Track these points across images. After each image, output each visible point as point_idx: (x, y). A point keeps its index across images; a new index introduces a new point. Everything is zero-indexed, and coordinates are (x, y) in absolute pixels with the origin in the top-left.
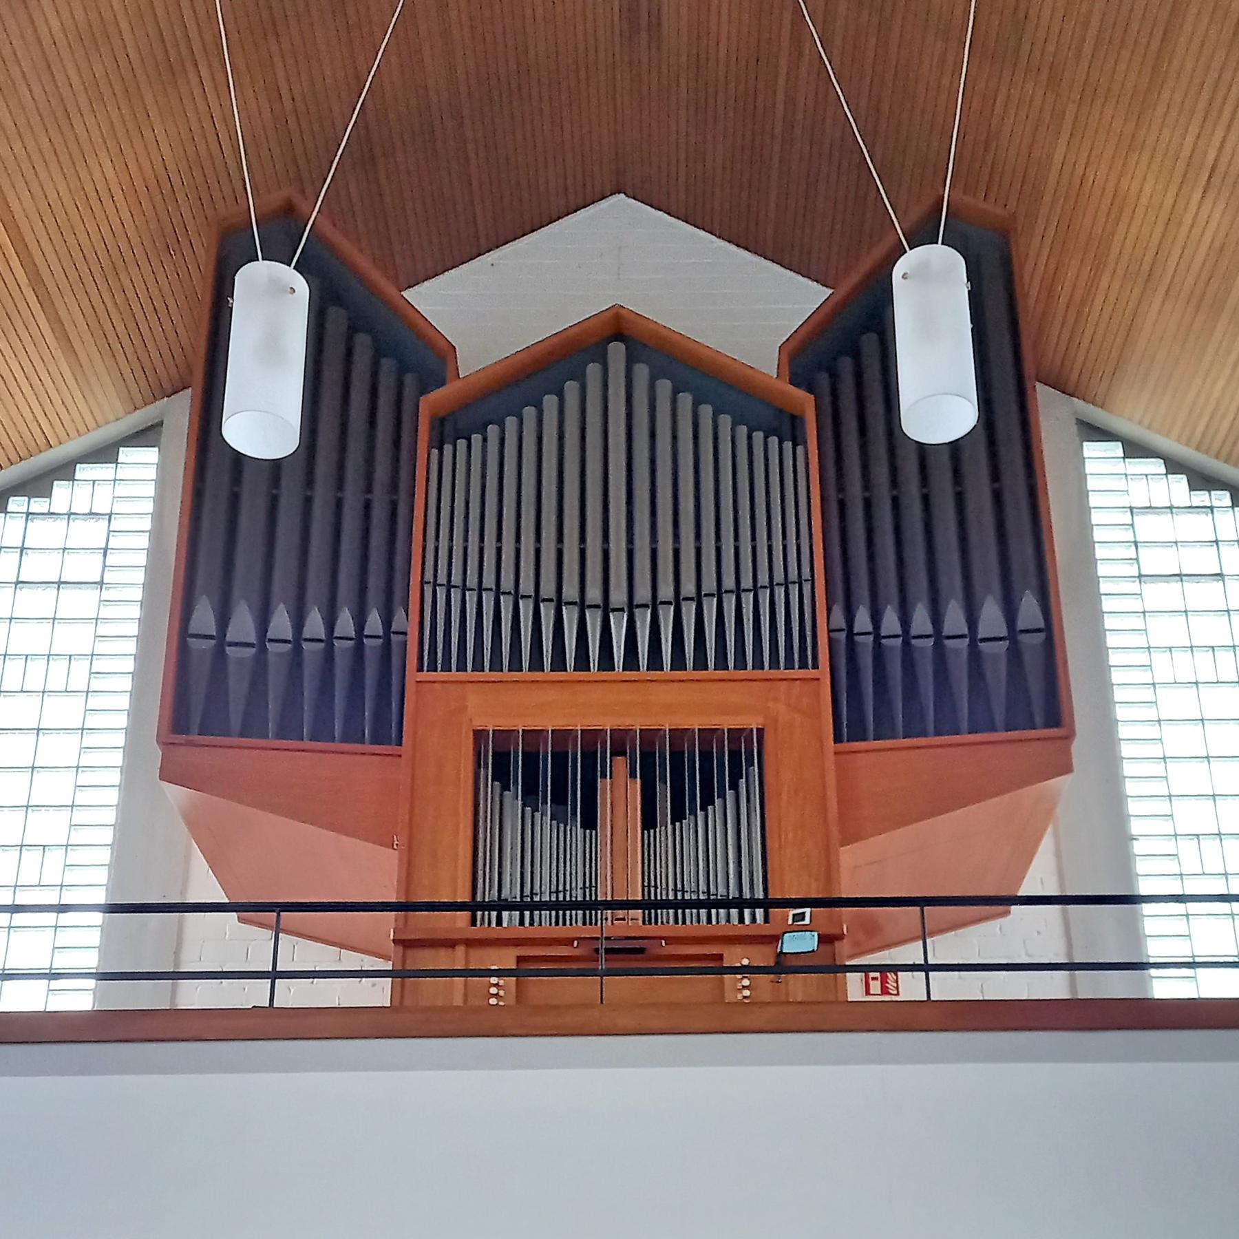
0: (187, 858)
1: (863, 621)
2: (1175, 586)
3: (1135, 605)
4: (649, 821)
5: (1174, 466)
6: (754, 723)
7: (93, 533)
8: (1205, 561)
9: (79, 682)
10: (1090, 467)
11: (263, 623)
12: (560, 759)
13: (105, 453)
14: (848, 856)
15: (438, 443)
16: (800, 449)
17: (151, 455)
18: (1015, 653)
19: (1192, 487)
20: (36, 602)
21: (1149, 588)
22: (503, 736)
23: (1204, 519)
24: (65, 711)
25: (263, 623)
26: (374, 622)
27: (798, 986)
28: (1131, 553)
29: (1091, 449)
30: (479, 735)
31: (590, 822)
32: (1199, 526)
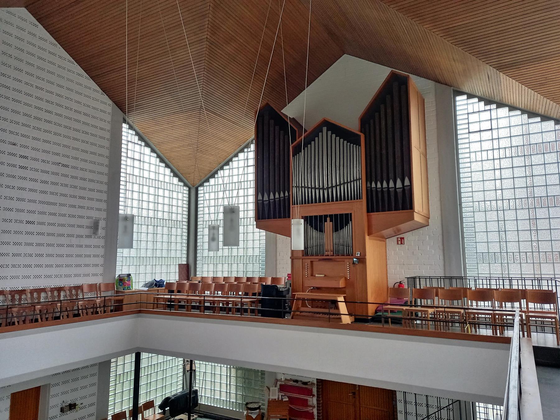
1: (373, 185)
4: (333, 232)
16: (360, 147)
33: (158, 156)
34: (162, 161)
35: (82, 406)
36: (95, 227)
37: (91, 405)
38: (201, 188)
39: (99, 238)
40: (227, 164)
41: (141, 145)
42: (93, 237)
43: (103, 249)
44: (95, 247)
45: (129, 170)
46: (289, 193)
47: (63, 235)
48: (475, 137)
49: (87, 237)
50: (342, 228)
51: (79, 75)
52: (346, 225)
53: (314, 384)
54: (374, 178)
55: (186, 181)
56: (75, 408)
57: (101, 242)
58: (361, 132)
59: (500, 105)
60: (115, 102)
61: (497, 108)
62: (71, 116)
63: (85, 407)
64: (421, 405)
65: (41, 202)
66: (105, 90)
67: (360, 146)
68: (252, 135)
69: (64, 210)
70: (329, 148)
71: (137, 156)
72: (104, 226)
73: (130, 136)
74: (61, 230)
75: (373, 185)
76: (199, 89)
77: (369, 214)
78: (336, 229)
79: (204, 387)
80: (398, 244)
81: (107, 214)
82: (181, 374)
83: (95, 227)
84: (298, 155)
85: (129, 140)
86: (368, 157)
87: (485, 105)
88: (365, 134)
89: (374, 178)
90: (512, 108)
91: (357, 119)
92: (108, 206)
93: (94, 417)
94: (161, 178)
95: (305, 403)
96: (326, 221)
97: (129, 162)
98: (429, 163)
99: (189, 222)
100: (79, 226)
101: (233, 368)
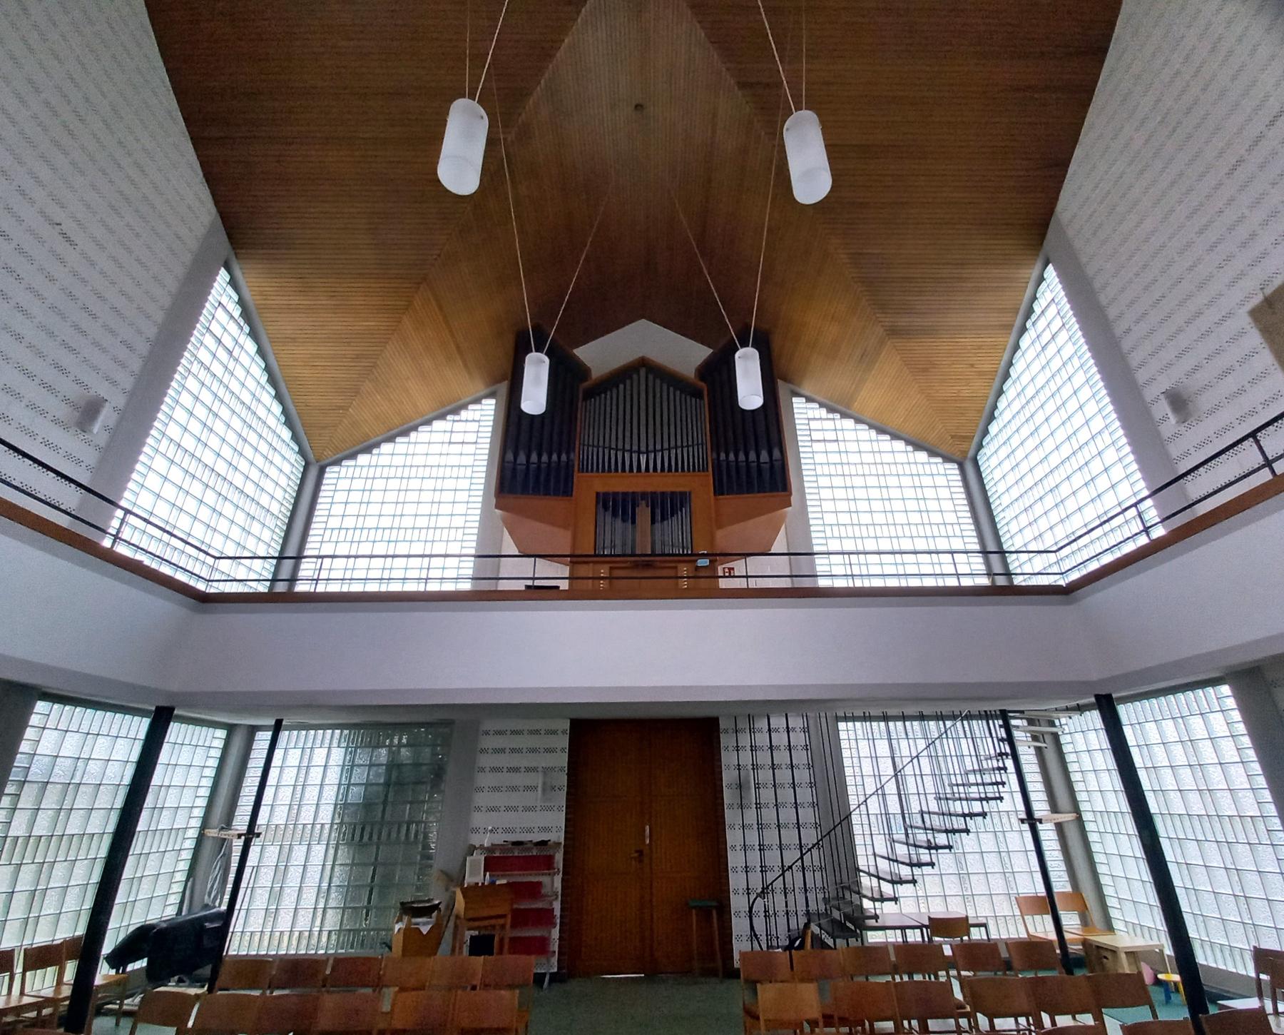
0: (503, 531)
1: (723, 456)
3: (810, 450)
4: (653, 522)
5: (822, 405)
6: (687, 489)
7: (474, 426)
8: (831, 436)
9: (469, 475)
10: (795, 405)
11: (528, 457)
12: (624, 500)
13: (477, 401)
14: (720, 534)
15: (585, 399)
17: (493, 401)
18: (772, 467)
19: (828, 412)
20: (456, 449)
21: (814, 444)
22: (606, 494)
23: (832, 422)
24: (464, 484)
25: (528, 457)
26: (564, 457)
27: (703, 583)
28: (808, 433)
29: (795, 400)
30: (598, 494)
31: (634, 522)
32: (829, 424)
34: (272, 381)
40: (405, 433)
53: (561, 843)
64: (770, 847)
82: (181, 877)
91: (694, 371)
92: (128, 404)
95: (534, 890)
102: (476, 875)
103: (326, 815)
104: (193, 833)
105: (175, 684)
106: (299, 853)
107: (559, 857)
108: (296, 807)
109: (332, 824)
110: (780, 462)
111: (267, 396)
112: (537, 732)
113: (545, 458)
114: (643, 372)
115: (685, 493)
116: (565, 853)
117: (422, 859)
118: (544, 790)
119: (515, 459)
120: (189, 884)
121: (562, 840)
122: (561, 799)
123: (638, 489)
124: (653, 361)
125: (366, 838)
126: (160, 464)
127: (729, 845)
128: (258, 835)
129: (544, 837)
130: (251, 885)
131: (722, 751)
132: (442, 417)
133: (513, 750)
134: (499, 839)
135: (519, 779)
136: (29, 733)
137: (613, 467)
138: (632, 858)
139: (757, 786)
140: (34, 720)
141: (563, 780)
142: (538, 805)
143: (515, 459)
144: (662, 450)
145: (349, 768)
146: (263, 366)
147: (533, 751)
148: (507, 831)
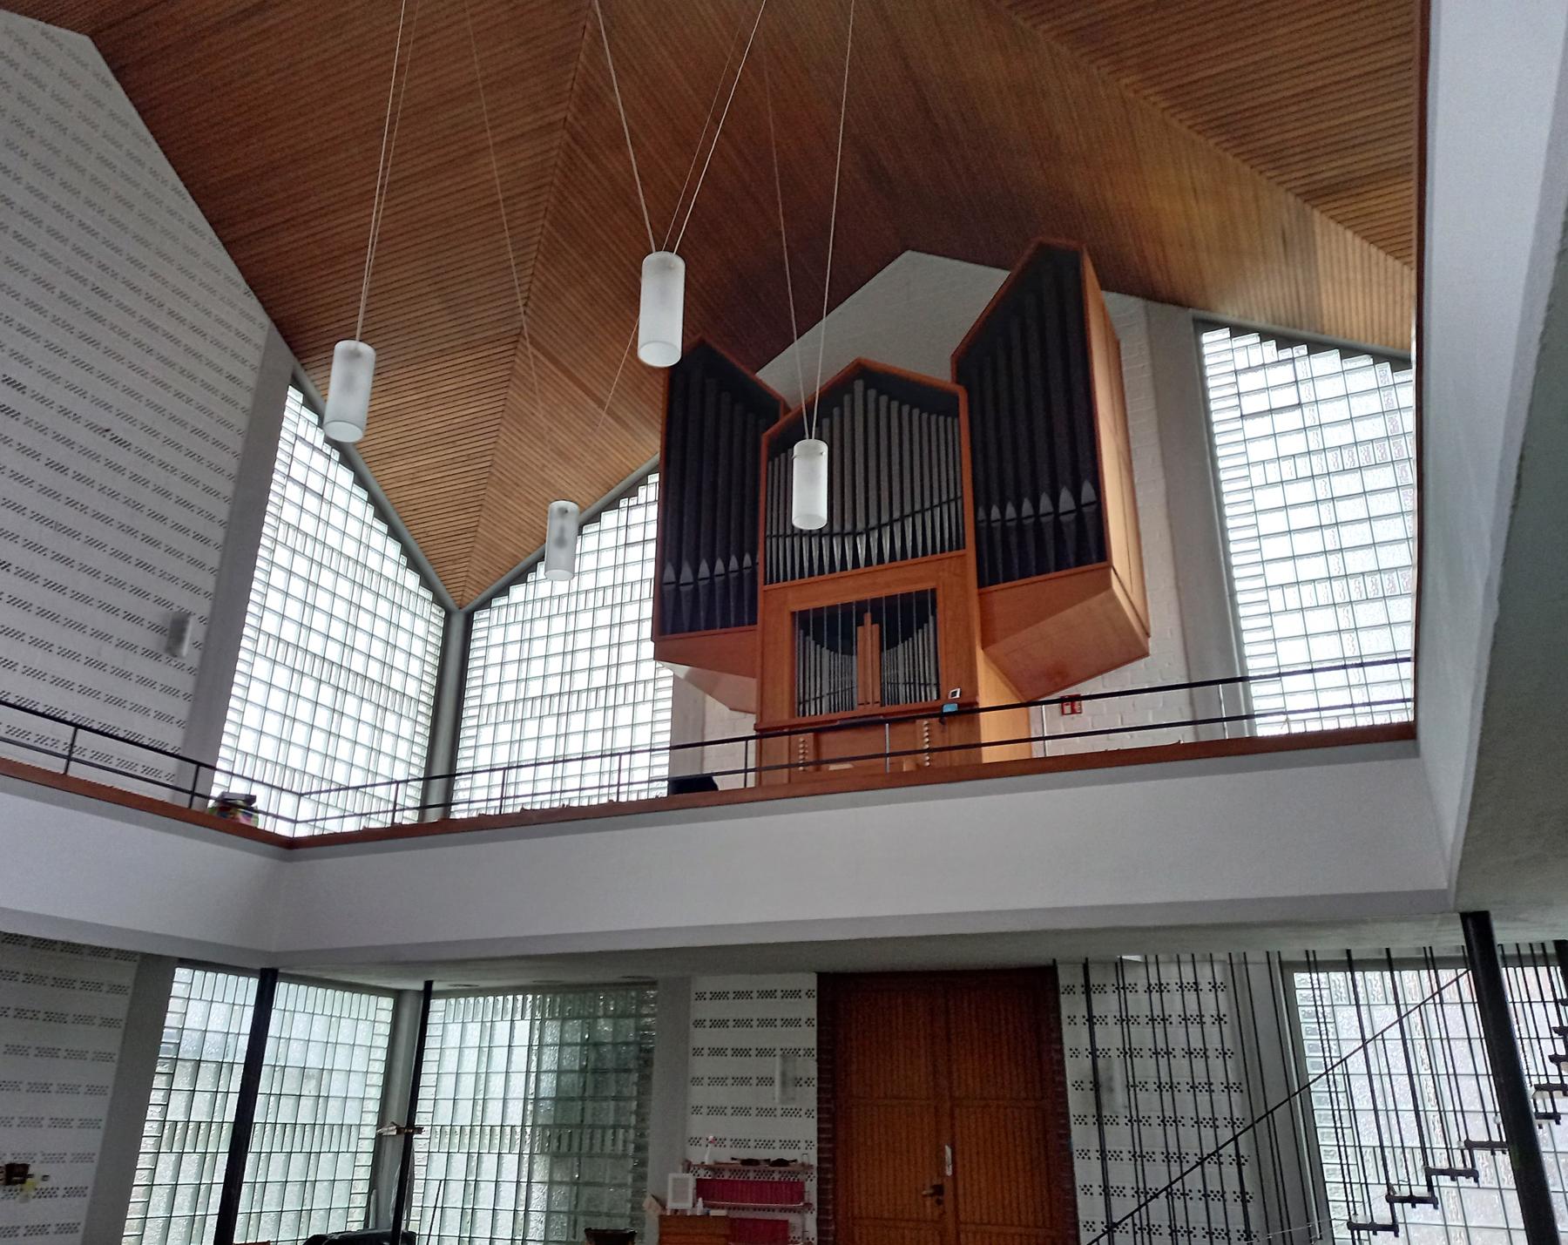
2: (1267, 419)
4: (881, 650)
5: (1265, 336)
6: (928, 586)
21: (1248, 423)
22: (803, 614)
32: (1284, 374)
33: (373, 500)
34: (381, 514)
35: (43, 1185)
36: (175, 631)
37: (71, 1192)
38: (481, 620)
39: (180, 667)
41: (329, 457)
42: (163, 658)
43: (186, 703)
44: (166, 690)
45: (290, 514)
46: (753, 558)
47: (81, 628)
48: (1255, 427)
49: (147, 653)
50: (907, 635)
51: (192, 227)
52: (920, 626)
54: (995, 496)
55: (441, 587)
56: (23, 1182)
57: (186, 683)
58: (958, 382)
59: (1316, 347)
60: (279, 324)
61: (1309, 354)
62: (158, 323)
63: (50, 1193)
65: (39, 518)
66: (256, 284)
67: (958, 416)
68: (651, 447)
69: (97, 559)
70: (872, 441)
71: (315, 483)
72: (200, 638)
73: (302, 424)
74: (80, 612)
75: (995, 513)
76: (518, 290)
77: (983, 590)
78: (889, 641)
79: (435, 1232)
80: (1063, 713)
81: (214, 607)
82: (362, 1187)
83: (175, 631)
84: (783, 455)
85: (301, 433)
86: (979, 456)
87: (1279, 348)
88: (969, 391)
89: (995, 496)
90: (1348, 351)
93: (77, 1238)
94: (373, 561)
96: (860, 623)
97: (293, 492)
98: (1139, 494)
99: (437, 708)
100: (129, 617)
101: (542, 1153)
102: (685, 1201)
103: (515, 1117)
104: (370, 1132)
105: (274, 941)
106: (489, 1162)
107: (811, 1187)
108: (481, 1102)
109: (523, 1126)
110: (1094, 507)
111: (378, 537)
112: (770, 994)
113: (719, 566)
114: (859, 386)
115: (925, 592)
116: (821, 1181)
117: (634, 1180)
118: (784, 1084)
119: (678, 577)
120: (373, 1197)
121: (814, 1161)
122: (809, 1097)
123: (853, 598)
124: (875, 363)
125: (564, 1148)
126: (262, 669)
127: (1079, 1183)
128: (420, 1130)
129: (788, 1155)
130: (439, 1205)
131: (1065, 1027)
132: (613, 505)
133: (738, 1023)
134: (725, 1155)
135: (752, 1067)
136: (174, 1005)
137: (806, 570)
138: (925, 1196)
139: (1131, 1086)
140: (177, 989)
141: (810, 1068)
142: (779, 1107)
143: (678, 577)
144: (940, 505)
145: (536, 1048)
146: (365, 497)
147: (767, 1023)
148: (737, 1143)
